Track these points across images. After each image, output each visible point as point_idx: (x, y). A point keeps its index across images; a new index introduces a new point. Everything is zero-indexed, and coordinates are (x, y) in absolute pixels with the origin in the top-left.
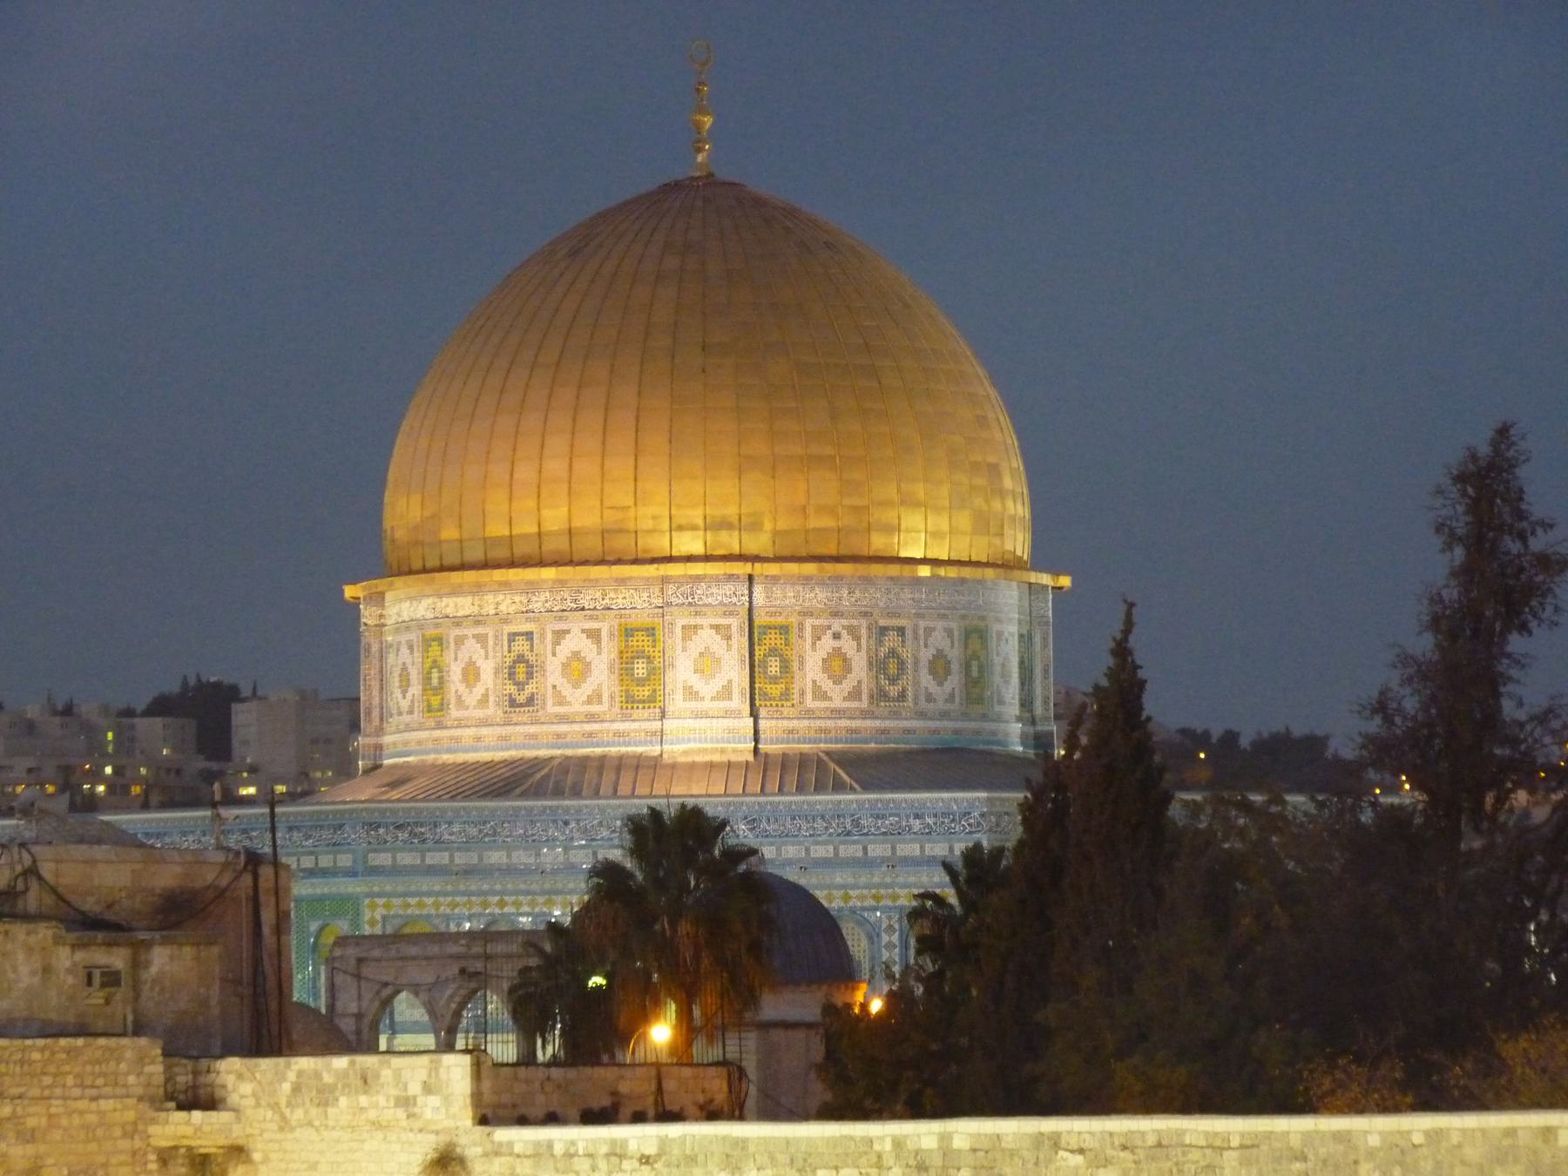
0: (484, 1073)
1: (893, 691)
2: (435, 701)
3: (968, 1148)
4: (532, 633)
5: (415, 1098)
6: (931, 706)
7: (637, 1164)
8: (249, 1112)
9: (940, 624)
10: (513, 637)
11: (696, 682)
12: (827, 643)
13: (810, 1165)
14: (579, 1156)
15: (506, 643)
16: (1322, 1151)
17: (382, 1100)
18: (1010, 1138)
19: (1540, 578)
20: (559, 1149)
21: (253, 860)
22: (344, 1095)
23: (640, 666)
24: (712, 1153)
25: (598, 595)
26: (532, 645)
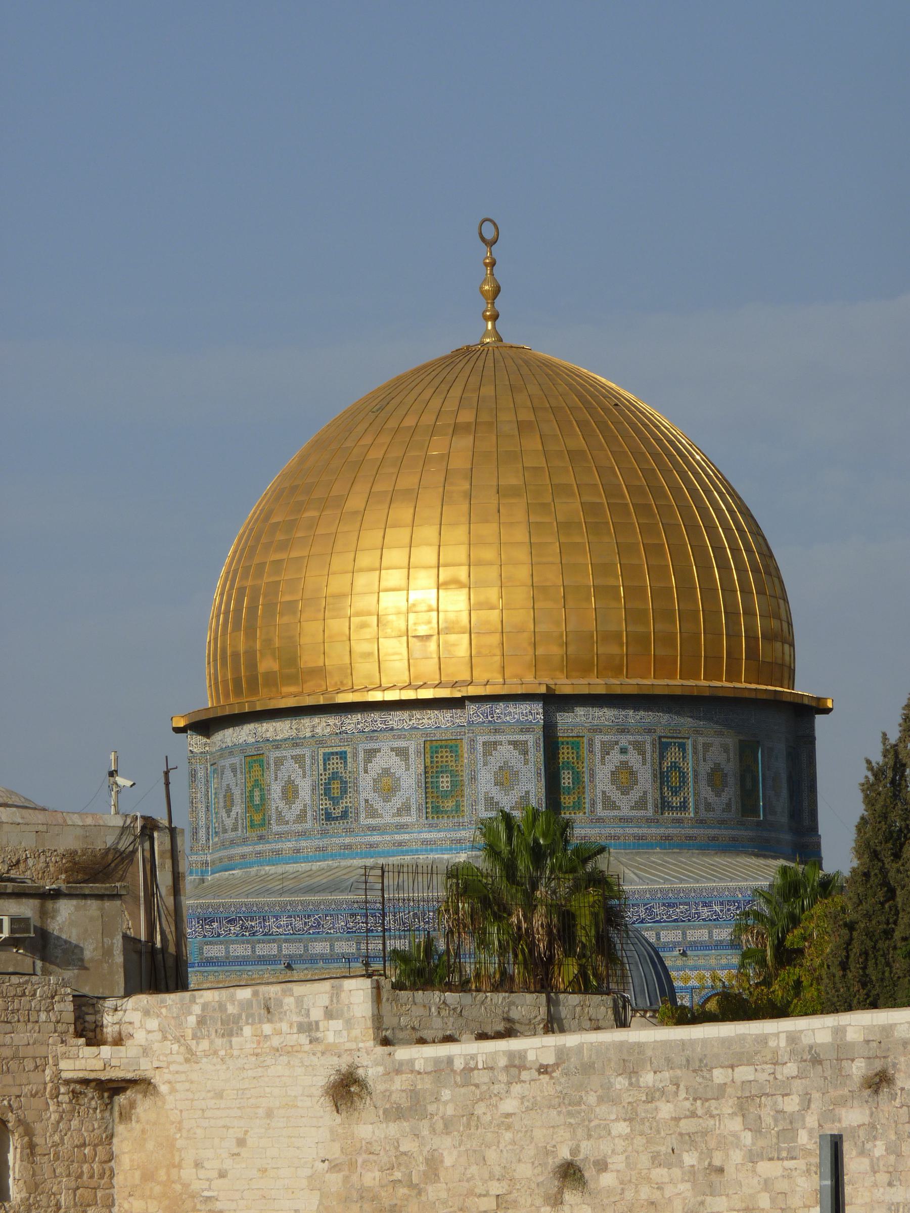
0: (385, 995)
1: (676, 801)
2: (257, 818)
4: (345, 752)
5: (317, 1023)
6: (711, 815)
7: (535, 1074)
8: (156, 1046)
9: (717, 741)
12: (615, 757)
13: (706, 1065)
14: (478, 1069)
15: (321, 762)
20: (459, 1064)
21: (149, 826)
22: (248, 1024)
23: (445, 780)
24: (609, 1060)
26: (345, 762)
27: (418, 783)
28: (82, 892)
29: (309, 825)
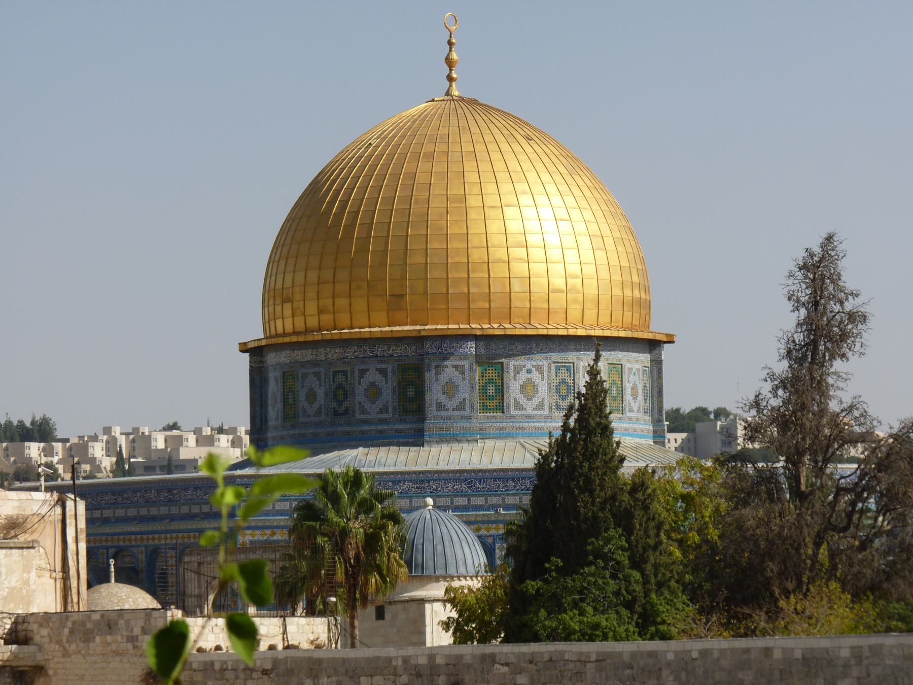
3: (444, 663)
4: (347, 371)
7: (260, 675)
8: (46, 646)
10: (335, 373)
11: (443, 399)
12: (523, 376)
13: (357, 674)
15: (331, 377)
16: (641, 663)
17: (119, 638)
18: (468, 657)
19: (850, 327)
20: (217, 666)
25: (385, 348)
26: (347, 377)
27: (394, 392)
28: (9, 546)
29: (323, 418)
